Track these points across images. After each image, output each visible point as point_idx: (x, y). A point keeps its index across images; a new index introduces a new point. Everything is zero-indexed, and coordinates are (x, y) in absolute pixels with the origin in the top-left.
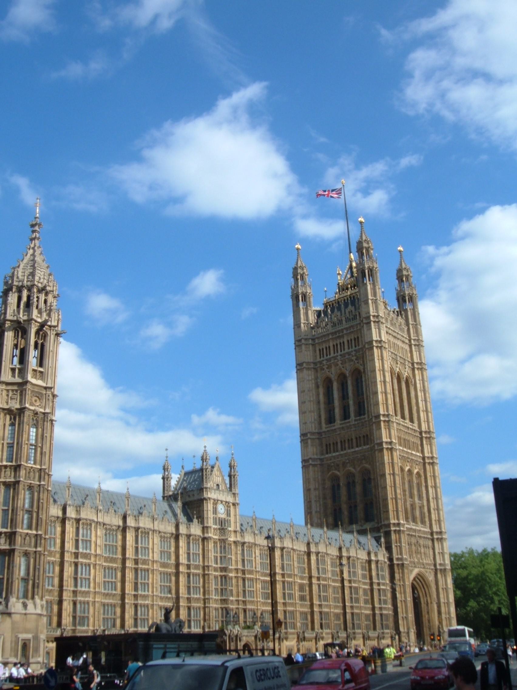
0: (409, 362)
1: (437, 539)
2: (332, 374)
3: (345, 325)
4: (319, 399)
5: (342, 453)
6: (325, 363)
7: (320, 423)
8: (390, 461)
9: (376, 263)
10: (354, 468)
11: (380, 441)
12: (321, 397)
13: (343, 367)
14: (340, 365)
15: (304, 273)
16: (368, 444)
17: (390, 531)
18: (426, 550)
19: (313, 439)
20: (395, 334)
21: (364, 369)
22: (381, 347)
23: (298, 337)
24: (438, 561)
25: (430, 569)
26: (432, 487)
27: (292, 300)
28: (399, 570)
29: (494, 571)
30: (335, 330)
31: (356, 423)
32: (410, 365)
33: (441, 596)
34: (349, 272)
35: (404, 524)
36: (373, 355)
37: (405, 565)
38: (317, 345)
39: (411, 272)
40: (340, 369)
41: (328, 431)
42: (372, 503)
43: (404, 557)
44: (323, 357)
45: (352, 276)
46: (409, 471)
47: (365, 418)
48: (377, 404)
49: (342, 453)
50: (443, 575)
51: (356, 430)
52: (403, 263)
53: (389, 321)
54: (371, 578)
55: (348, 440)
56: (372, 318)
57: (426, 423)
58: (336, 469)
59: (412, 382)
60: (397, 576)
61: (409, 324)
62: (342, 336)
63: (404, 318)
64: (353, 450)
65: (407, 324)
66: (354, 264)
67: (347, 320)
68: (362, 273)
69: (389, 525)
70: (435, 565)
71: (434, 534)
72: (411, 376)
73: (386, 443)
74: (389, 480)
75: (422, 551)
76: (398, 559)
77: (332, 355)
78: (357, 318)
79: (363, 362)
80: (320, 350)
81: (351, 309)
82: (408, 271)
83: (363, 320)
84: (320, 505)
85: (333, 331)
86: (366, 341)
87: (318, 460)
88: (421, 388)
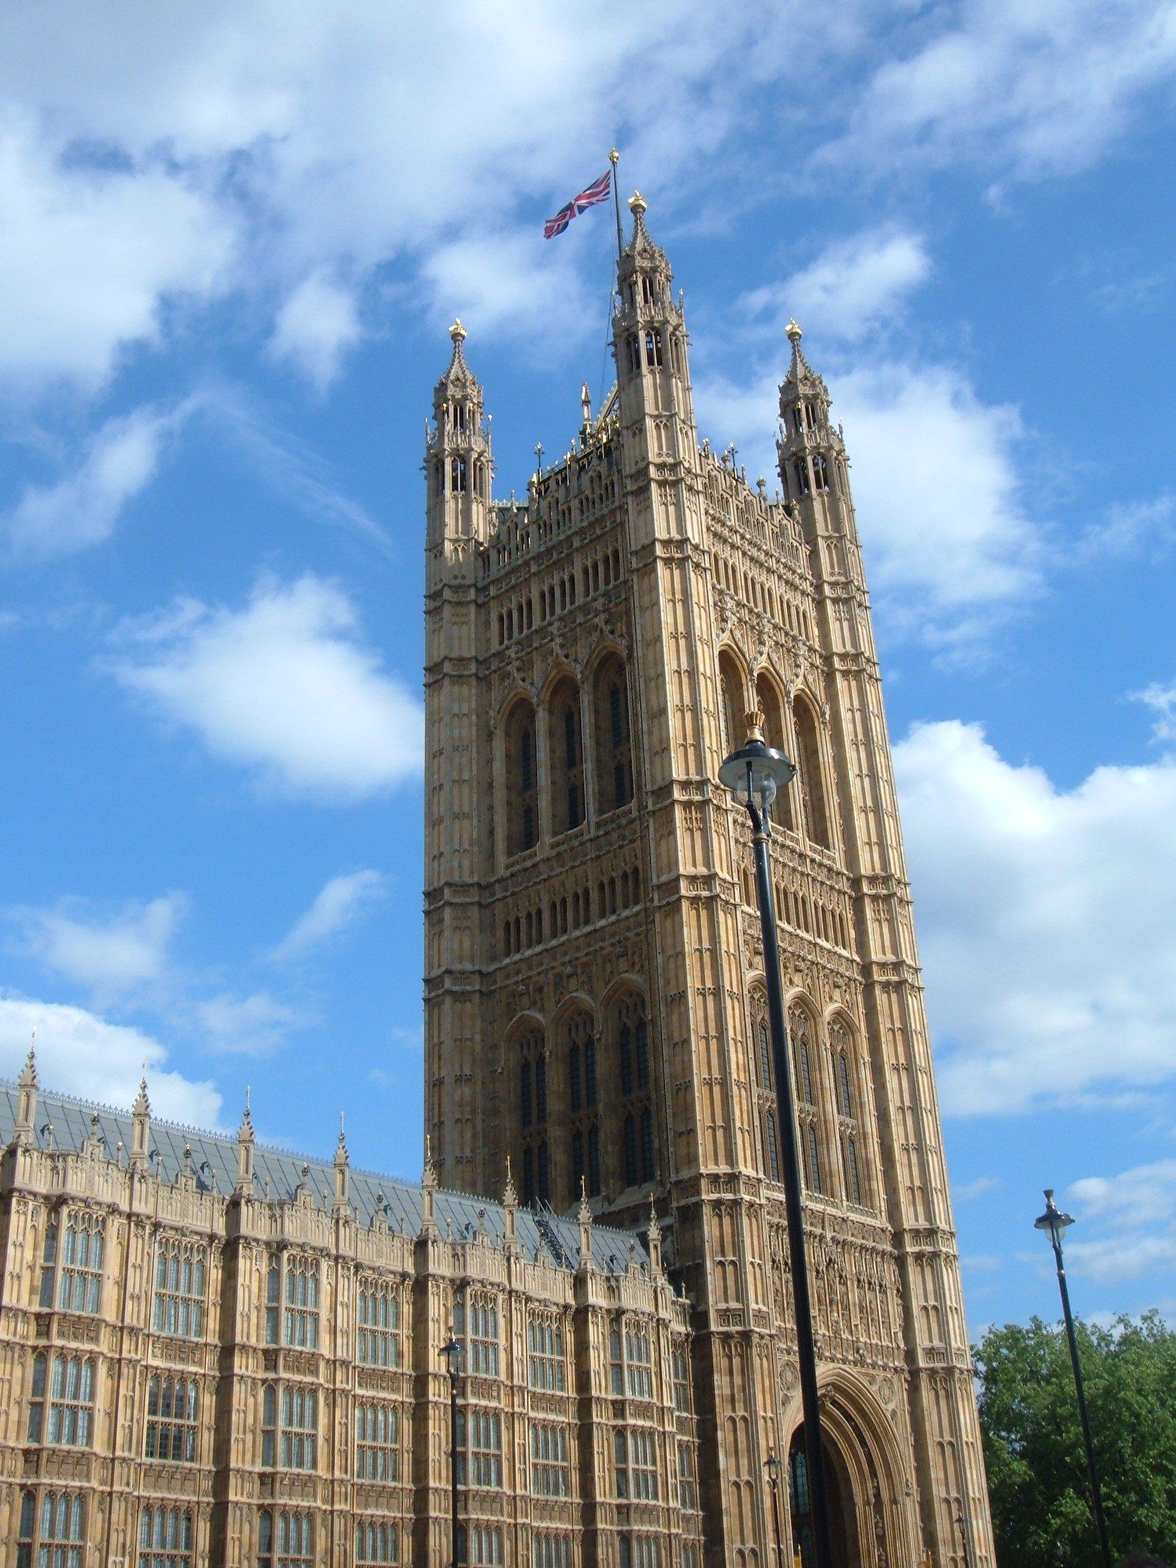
0: (810, 649)
1: (919, 1257)
2: (532, 684)
3: (577, 521)
4: (491, 773)
5: (554, 943)
7: (491, 856)
8: (706, 945)
10: (591, 992)
11: (672, 875)
13: (567, 656)
14: (557, 650)
16: (636, 902)
17: (698, 1205)
18: (869, 1295)
19: (464, 906)
20: (754, 552)
21: (630, 649)
23: (436, 584)
24: (922, 1341)
25: (885, 1368)
26: (896, 1069)
28: (730, 1358)
29: (1150, 1385)
30: (550, 544)
32: (818, 662)
33: (936, 1474)
35: (759, 1180)
36: (654, 588)
37: (755, 1339)
38: (492, 604)
40: (558, 664)
41: (513, 875)
42: (646, 1114)
43: (753, 1306)
46: (801, 1001)
48: (663, 750)
49: (554, 943)
50: (942, 1393)
51: (598, 857)
54: (583, 1382)
55: (576, 896)
56: (653, 472)
57: (875, 849)
58: (533, 1004)
59: (823, 714)
60: (721, 1383)
62: (569, 559)
63: (798, 518)
65: (810, 538)
67: (586, 504)
69: (692, 1185)
70: (910, 1356)
71: (907, 1238)
73: (693, 879)
74: (700, 1013)
75: (854, 1296)
76: (725, 1315)
77: (537, 623)
78: (613, 495)
79: (629, 625)
80: (501, 618)
82: (813, 385)
84: (474, 1136)
87: (477, 977)
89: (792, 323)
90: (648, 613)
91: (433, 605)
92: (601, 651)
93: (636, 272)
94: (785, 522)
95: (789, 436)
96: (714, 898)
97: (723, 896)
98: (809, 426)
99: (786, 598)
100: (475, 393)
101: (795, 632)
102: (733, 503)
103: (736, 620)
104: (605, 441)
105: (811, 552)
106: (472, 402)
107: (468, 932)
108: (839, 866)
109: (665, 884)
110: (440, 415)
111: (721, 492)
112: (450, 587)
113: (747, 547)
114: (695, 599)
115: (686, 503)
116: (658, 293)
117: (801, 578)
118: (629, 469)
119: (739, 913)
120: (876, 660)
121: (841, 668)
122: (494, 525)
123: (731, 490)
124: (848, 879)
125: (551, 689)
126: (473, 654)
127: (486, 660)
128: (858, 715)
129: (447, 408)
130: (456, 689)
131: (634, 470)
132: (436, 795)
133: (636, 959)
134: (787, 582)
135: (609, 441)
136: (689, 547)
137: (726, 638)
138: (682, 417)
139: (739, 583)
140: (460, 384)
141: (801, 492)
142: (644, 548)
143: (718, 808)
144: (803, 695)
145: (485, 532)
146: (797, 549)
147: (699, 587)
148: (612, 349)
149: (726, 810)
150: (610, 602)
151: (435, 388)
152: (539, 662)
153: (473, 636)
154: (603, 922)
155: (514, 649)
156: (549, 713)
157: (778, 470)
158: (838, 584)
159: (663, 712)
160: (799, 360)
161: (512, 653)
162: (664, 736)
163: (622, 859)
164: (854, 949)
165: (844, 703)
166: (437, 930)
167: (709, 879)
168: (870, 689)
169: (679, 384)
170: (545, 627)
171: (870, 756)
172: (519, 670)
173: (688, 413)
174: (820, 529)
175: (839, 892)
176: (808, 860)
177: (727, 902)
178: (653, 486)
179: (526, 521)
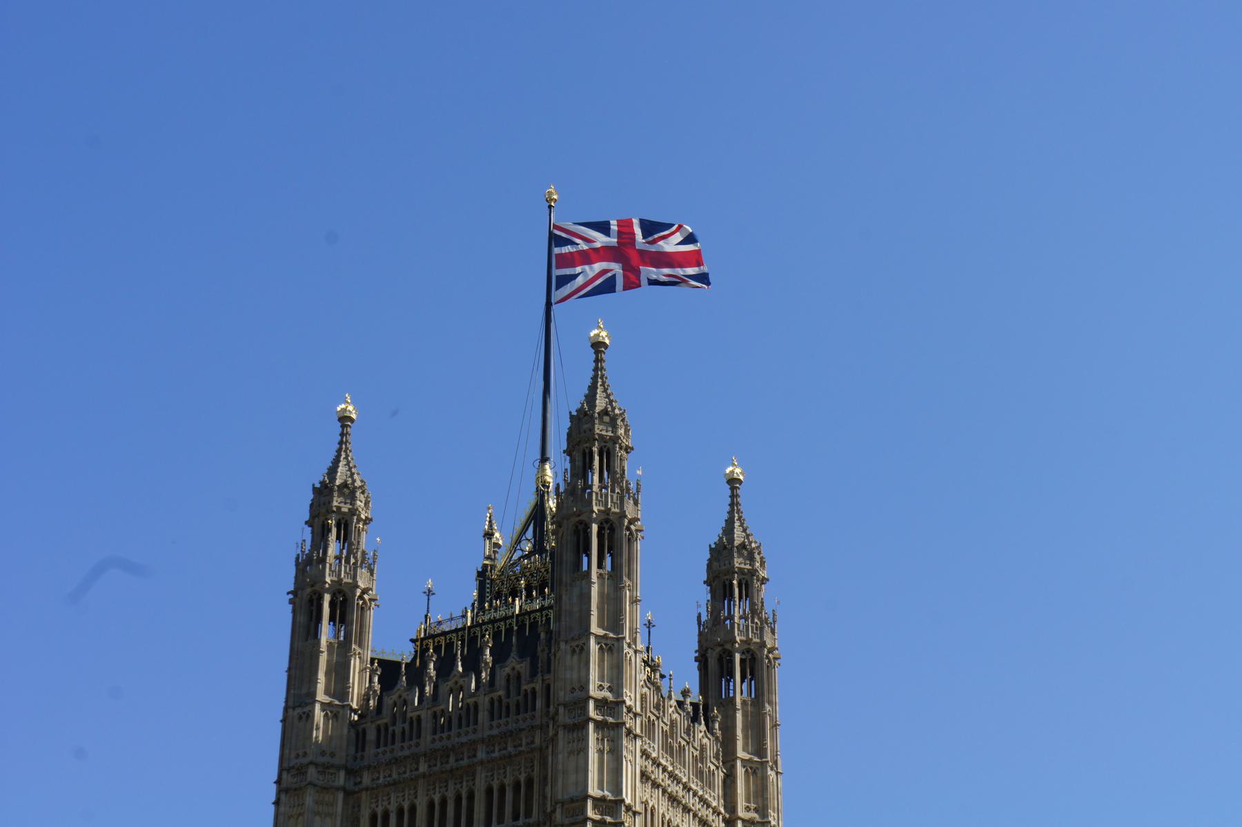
9: (636, 503)
23: (298, 756)
27: (294, 611)
34: (530, 534)
38: (364, 795)
39: (763, 563)
45: (539, 548)
52: (737, 524)
53: (658, 735)
61: (735, 758)
63: (719, 733)
65: (728, 758)
66: (552, 504)
68: (576, 532)
78: (534, 709)
81: (518, 667)
83: (557, 713)
85: (438, 745)
86: (560, 797)
94: (705, 741)
100: (362, 505)
112: (316, 765)
115: (624, 753)
118: (562, 695)
131: (569, 697)
142: (572, 800)
174: (741, 753)
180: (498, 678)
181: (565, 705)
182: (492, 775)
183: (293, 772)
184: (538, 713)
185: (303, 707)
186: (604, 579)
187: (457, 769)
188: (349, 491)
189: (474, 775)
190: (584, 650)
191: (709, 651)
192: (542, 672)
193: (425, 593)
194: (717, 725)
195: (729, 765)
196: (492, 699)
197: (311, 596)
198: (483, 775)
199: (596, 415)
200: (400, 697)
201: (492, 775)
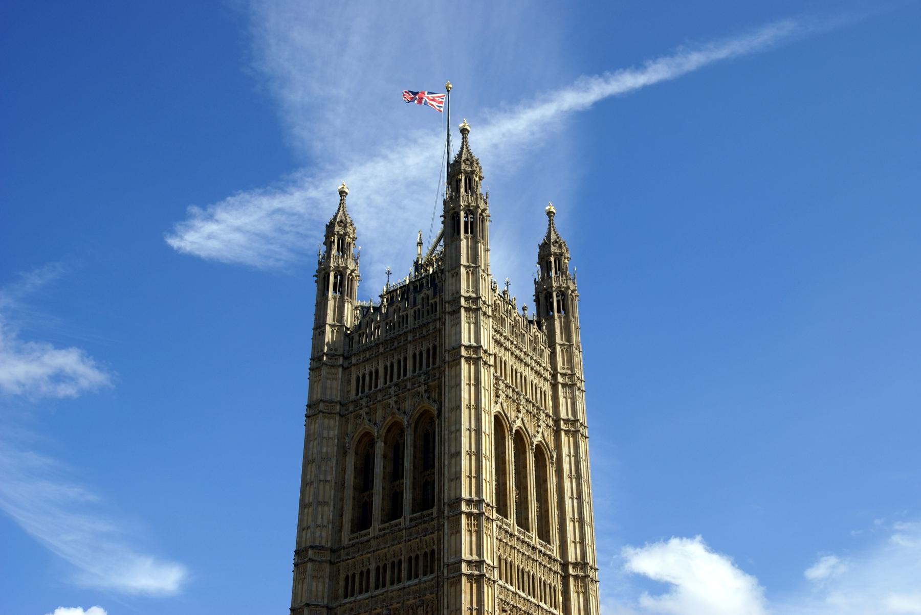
0: (547, 415)
4: (344, 478)
6: (364, 404)
8: (475, 606)
12: (350, 476)
13: (399, 409)
15: (346, 234)
16: (432, 572)
20: (518, 352)
22: (476, 361)
30: (392, 335)
31: (413, 523)
32: (551, 423)
40: (393, 414)
41: (353, 546)
44: (363, 392)
47: (432, 514)
59: (552, 457)
61: (555, 345)
63: (545, 331)
64: (401, 585)
65: (552, 344)
72: (552, 445)
73: (469, 563)
78: (436, 311)
79: (440, 394)
81: (427, 292)
86: (447, 348)
88: (571, 472)
89: (550, 205)
90: (453, 390)
91: (315, 365)
92: (420, 409)
93: (462, 172)
94: (537, 333)
95: (543, 278)
96: (482, 576)
97: (487, 575)
98: (556, 273)
99: (535, 382)
100: (352, 231)
101: (539, 404)
102: (508, 321)
103: (505, 396)
104: (431, 272)
105: (551, 353)
106: (349, 237)
107: (321, 580)
108: (555, 556)
109: (452, 564)
110: (328, 244)
111: (501, 314)
113: (514, 349)
114: (483, 385)
115: (482, 323)
116: (474, 188)
117: (544, 369)
118: (447, 298)
119: (496, 586)
120: (586, 425)
121: (565, 428)
122: (358, 318)
123: (507, 313)
124: (561, 564)
125: (387, 428)
126: (339, 399)
127: (346, 404)
128: (573, 459)
129: (334, 240)
130: (326, 421)
132: (308, 488)
133: (429, 610)
134: (536, 372)
135: (433, 273)
136: (482, 351)
137: (498, 408)
138: (483, 268)
139: (508, 372)
140: (343, 225)
141: (548, 313)
143: (488, 518)
144: (541, 444)
145: (351, 322)
146: (543, 351)
147: (486, 377)
148: (442, 219)
149: (492, 520)
150: (429, 378)
151: (327, 225)
152: (381, 411)
153: (339, 388)
154: (410, 583)
155: (365, 400)
156: (384, 443)
157: (534, 298)
158: (566, 375)
159: (459, 453)
160: (552, 229)
161: (363, 402)
162: (458, 469)
163: (425, 543)
164: (561, 610)
165: (565, 451)
166: (302, 577)
167: (480, 564)
168: (582, 443)
169: (482, 246)
170: (386, 388)
171: (579, 486)
172: (367, 413)
173: (487, 265)
174: (558, 339)
175: (555, 572)
176: (537, 551)
177: (489, 579)
178: (463, 310)
179: (378, 319)
180: (417, 299)
181: (449, 302)
182: (416, 348)
183: (316, 360)
184: (438, 313)
185: (321, 328)
186: (468, 239)
187: (398, 347)
188: (344, 224)
189: (406, 349)
190: (458, 274)
191: (540, 294)
192: (439, 292)
193: (386, 273)
194: (544, 327)
195: (552, 348)
196: (415, 310)
197: (325, 276)
198: (411, 348)
199: (462, 161)
200: (370, 318)
201: (416, 348)
